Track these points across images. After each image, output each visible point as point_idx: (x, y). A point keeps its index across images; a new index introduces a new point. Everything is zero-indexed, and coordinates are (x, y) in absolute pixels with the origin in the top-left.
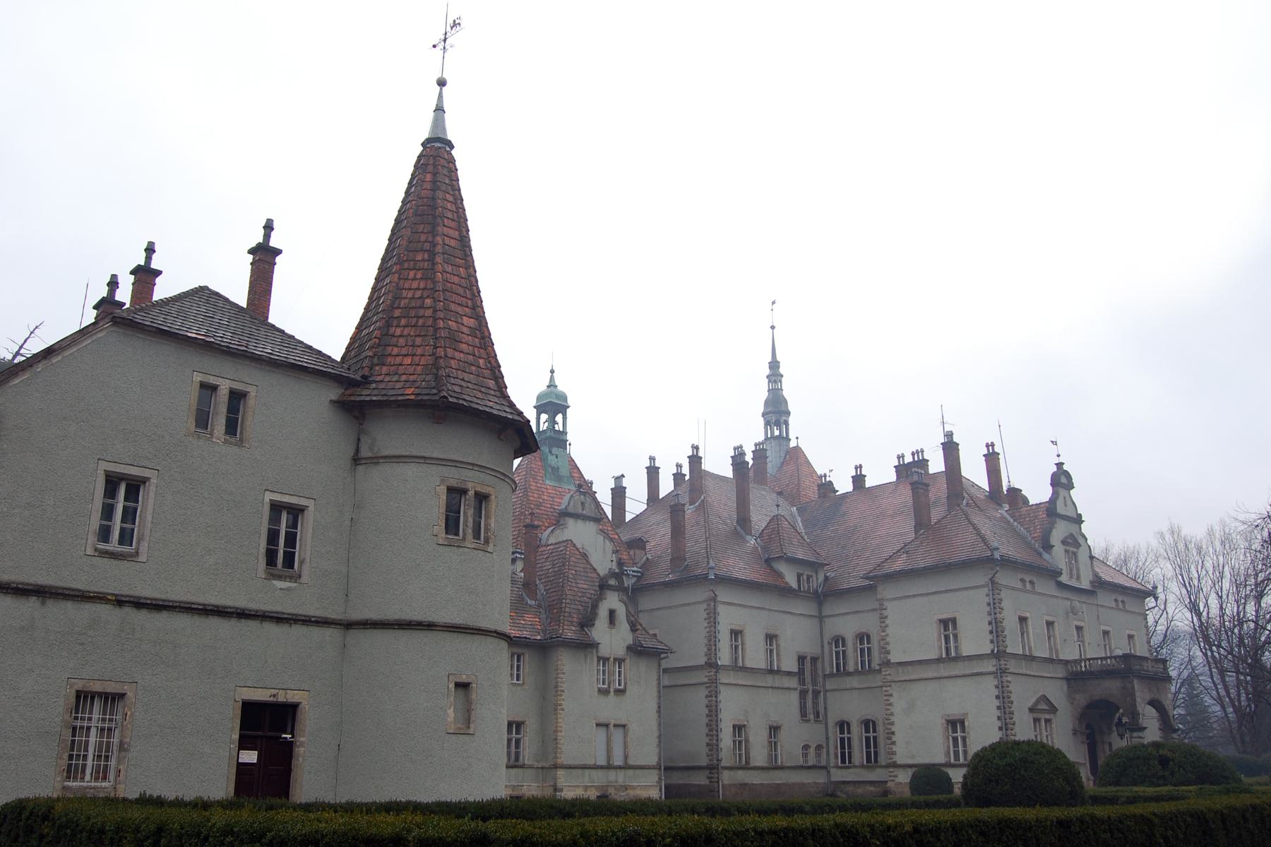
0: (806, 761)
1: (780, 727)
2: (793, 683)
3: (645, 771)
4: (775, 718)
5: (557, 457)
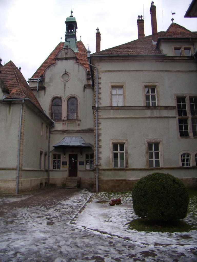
0: (188, 164)
1: (159, 143)
2: (174, 113)
3: (8, 171)
4: (152, 137)
5: (69, 42)
